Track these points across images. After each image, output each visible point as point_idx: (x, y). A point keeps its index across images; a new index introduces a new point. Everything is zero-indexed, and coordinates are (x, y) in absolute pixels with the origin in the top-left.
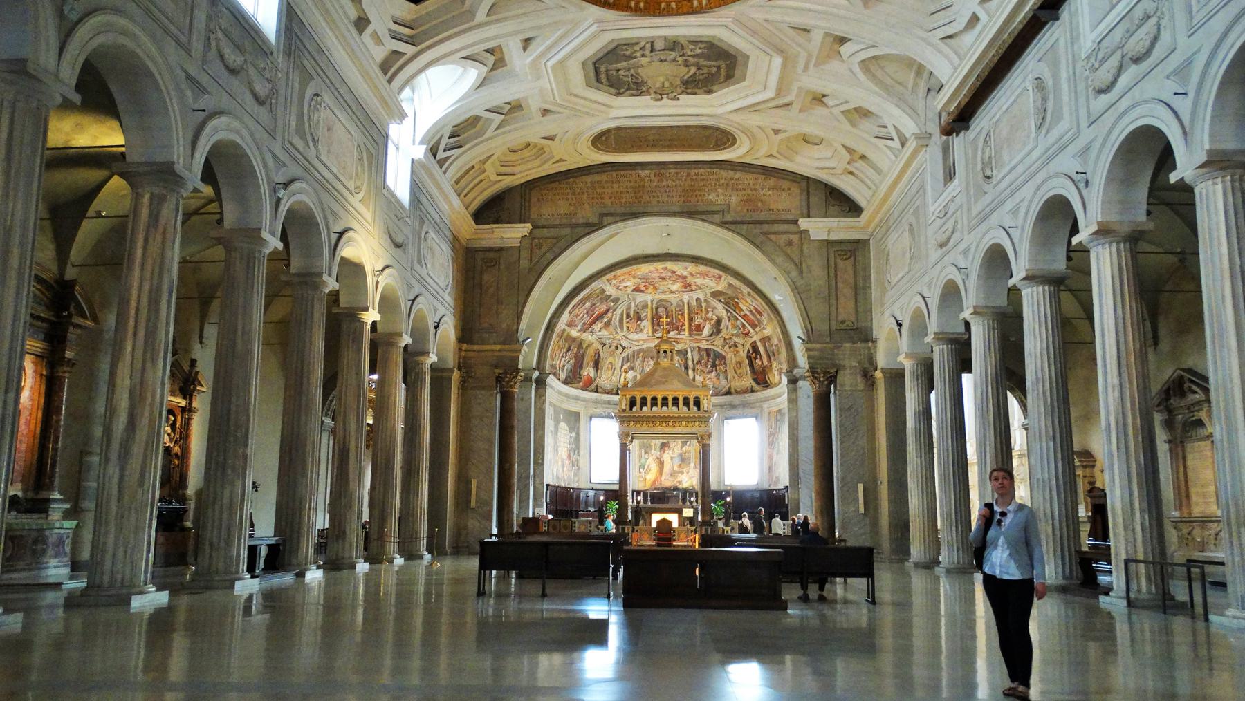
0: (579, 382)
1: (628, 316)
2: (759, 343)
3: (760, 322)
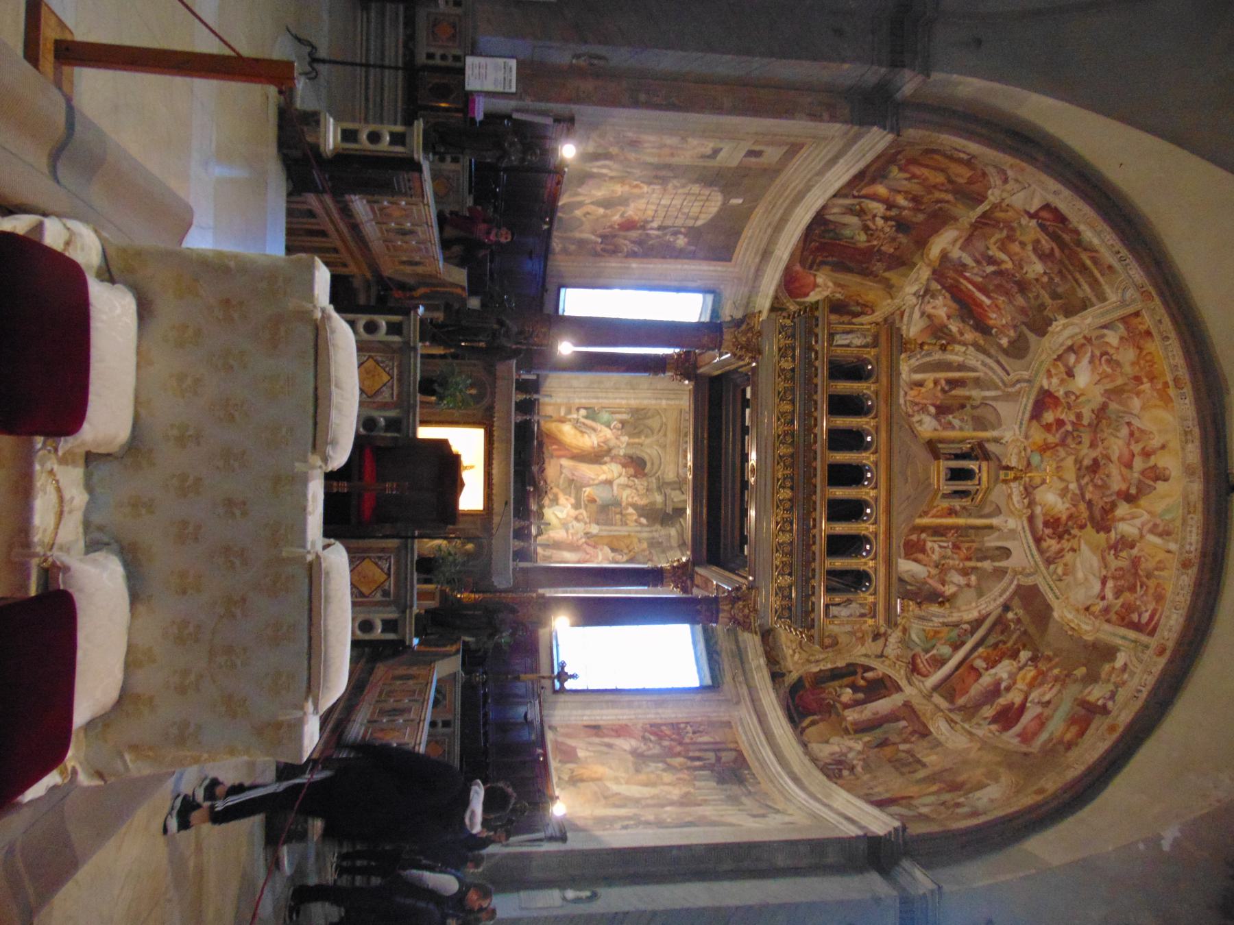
0: (803, 262)
1: (954, 383)
3: (970, 711)
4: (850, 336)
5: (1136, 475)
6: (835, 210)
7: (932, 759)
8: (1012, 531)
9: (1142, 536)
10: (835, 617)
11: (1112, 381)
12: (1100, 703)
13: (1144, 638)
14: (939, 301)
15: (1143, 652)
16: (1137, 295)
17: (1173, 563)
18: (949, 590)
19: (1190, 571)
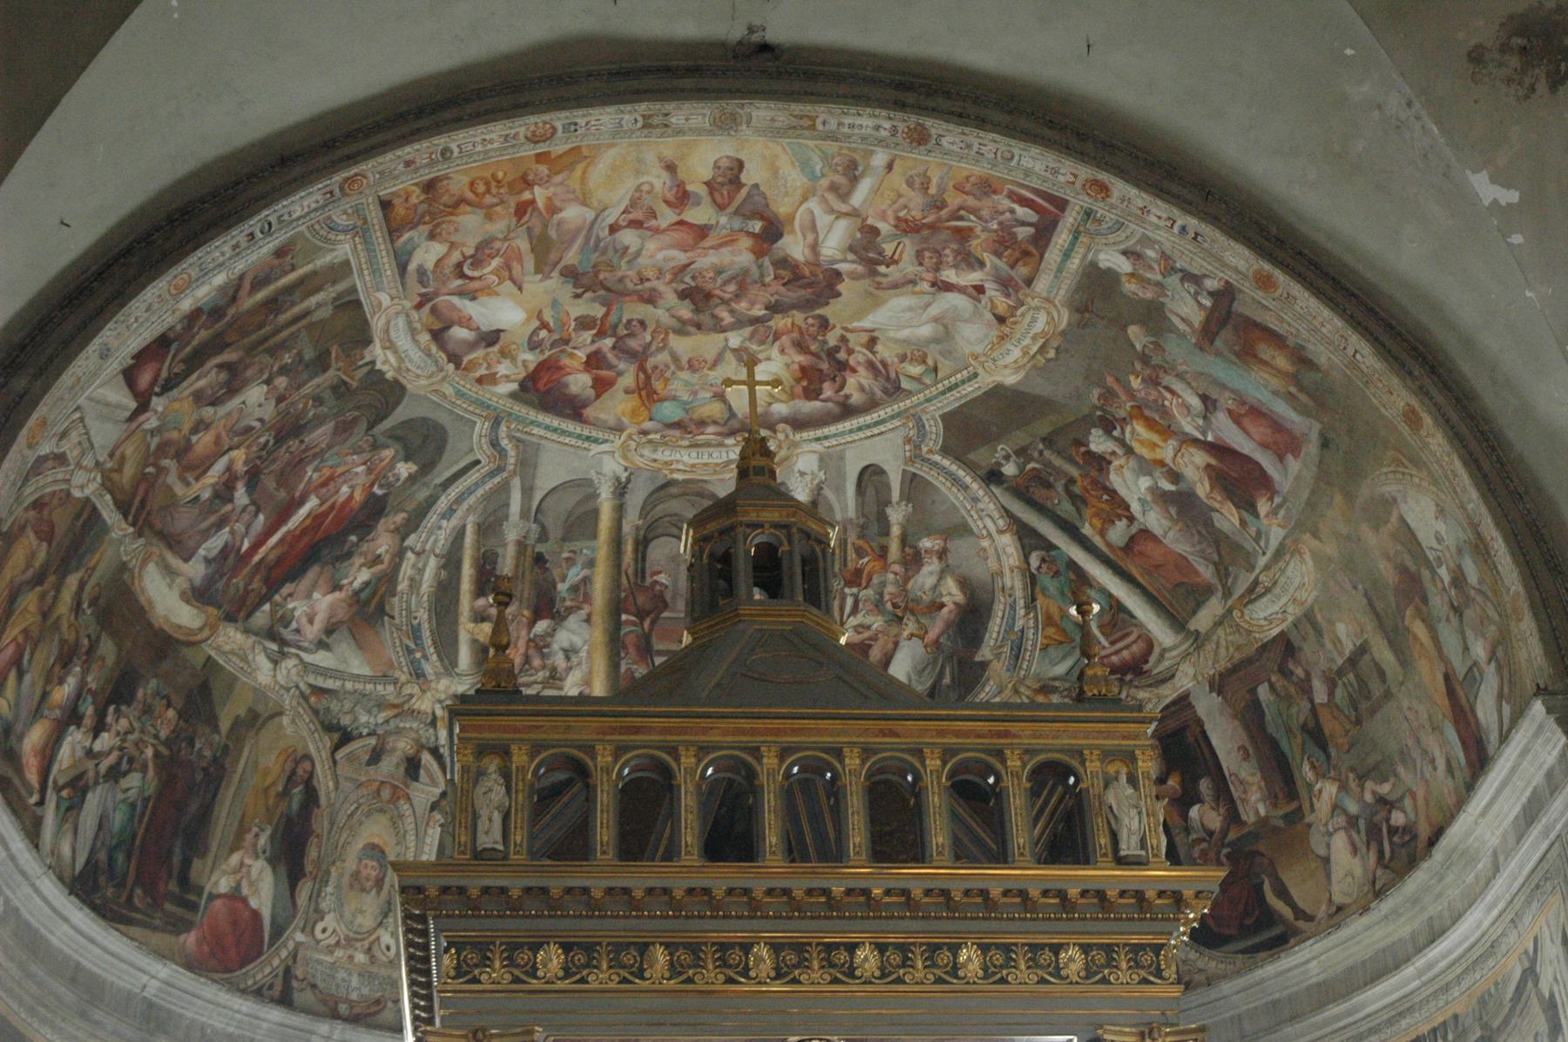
0: (178, 926)
1: (486, 580)
2: (1207, 706)
4: (484, 813)
5: (723, 220)
6: (66, 850)
7: (1345, 633)
8: (823, 461)
9: (854, 213)
10: (1143, 843)
11: (520, 260)
12: (1207, 302)
13: (1070, 219)
14: (298, 607)
15: (1099, 222)
16: (347, 204)
17: (914, 160)
18: (952, 593)
19: (933, 131)
